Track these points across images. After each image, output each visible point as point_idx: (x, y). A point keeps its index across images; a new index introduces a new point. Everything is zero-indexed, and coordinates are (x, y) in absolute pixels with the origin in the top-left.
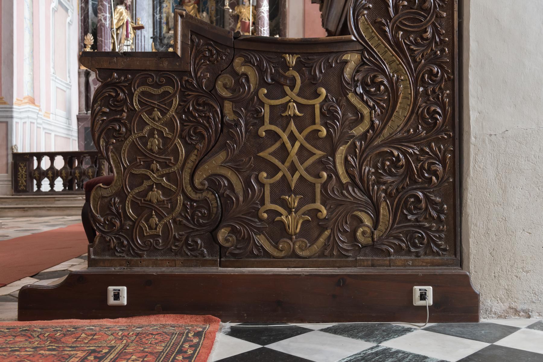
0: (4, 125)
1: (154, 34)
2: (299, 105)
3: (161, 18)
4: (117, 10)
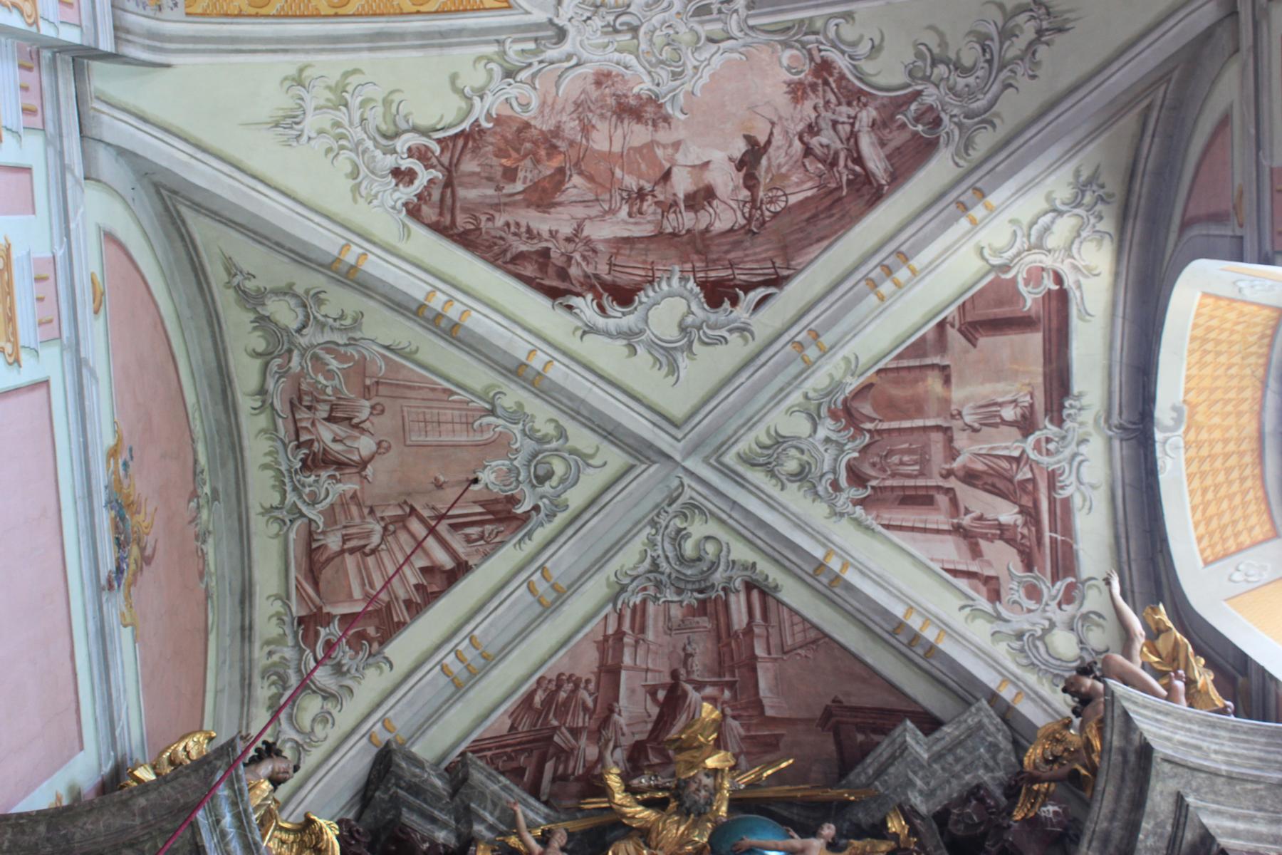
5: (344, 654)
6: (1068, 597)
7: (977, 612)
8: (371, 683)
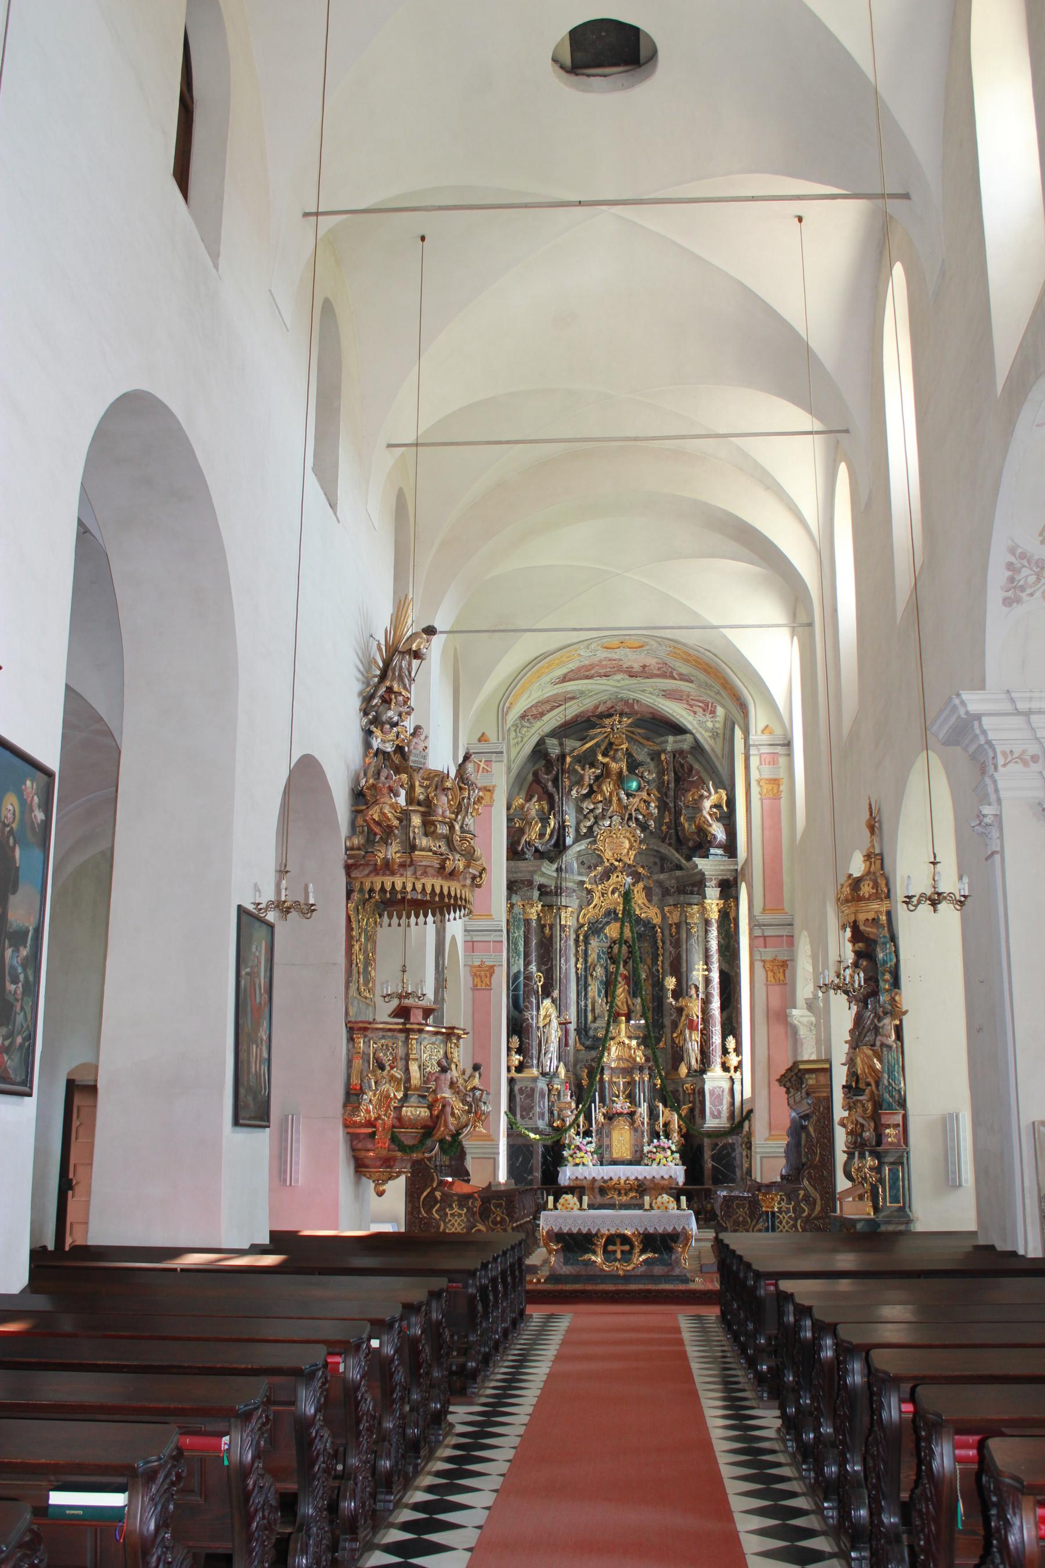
0: (492, 1160)
1: (578, 1026)
3: (586, 1006)
5: (532, 721)
6: (713, 717)
8: (539, 724)
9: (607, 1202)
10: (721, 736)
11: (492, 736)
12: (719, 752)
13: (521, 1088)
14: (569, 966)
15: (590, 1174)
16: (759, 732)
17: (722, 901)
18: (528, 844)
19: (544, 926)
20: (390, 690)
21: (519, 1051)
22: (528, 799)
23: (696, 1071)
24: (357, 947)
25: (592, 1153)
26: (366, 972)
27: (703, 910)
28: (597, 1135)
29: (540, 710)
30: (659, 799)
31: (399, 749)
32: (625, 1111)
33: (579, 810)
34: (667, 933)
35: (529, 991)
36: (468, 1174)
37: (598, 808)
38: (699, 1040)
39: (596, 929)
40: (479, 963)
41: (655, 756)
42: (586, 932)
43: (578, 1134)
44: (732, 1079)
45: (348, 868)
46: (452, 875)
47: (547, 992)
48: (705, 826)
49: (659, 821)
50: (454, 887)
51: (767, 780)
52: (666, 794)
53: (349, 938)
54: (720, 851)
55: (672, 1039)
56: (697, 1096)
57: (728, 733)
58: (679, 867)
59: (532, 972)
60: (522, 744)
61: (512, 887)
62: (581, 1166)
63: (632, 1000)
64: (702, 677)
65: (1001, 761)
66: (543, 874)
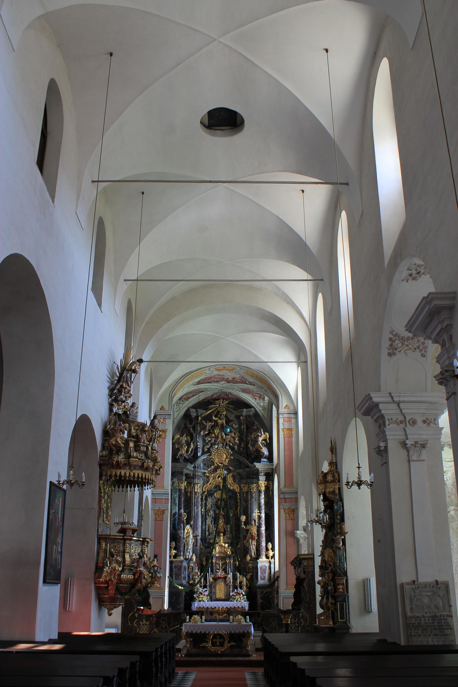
0: (162, 599)
1: (202, 537)
2: (294, 621)
3: (205, 528)
4: (187, 528)
5: (184, 401)
6: (263, 401)
7: (253, 400)
8: (187, 402)
9: (213, 618)
10: (267, 409)
11: (166, 407)
12: (266, 416)
13: (176, 565)
14: (198, 510)
15: (206, 605)
16: (283, 408)
17: (267, 482)
18: (181, 455)
19: (187, 492)
20: (122, 386)
21: (175, 549)
22: (182, 436)
23: (254, 558)
24: (103, 501)
25: (207, 596)
26: (107, 513)
27: (258, 486)
28: (209, 587)
29: (188, 396)
30: (239, 437)
31: (125, 413)
32: (222, 576)
33: (204, 441)
34: (242, 496)
35: (180, 521)
36: (150, 605)
37: (212, 440)
38: (255, 544)
39: (210, 494)
40: (158, 508)
41: (238, 417)
42: (206, 495)
43: (201, 587)
44: (270, 562)
45: (100, 465)
46: (147, 469)
47: (188, 522)
48: (259, 449)
49: (239, 446)
50: (147, 475)
51: (286, 429)
52: (242, 434)
53: (100, 497)
54: (265, 460)
55: (244, 543)
56: (254, 570)
57: (270, 408)
58: (248, 467)
59: (182, 513)
60: (179, 411)
61: (174, 474)
62: (202, 602)
63: (226, 526)
64: (259, 383)
65: (387, 423)
66: (188, 469)
